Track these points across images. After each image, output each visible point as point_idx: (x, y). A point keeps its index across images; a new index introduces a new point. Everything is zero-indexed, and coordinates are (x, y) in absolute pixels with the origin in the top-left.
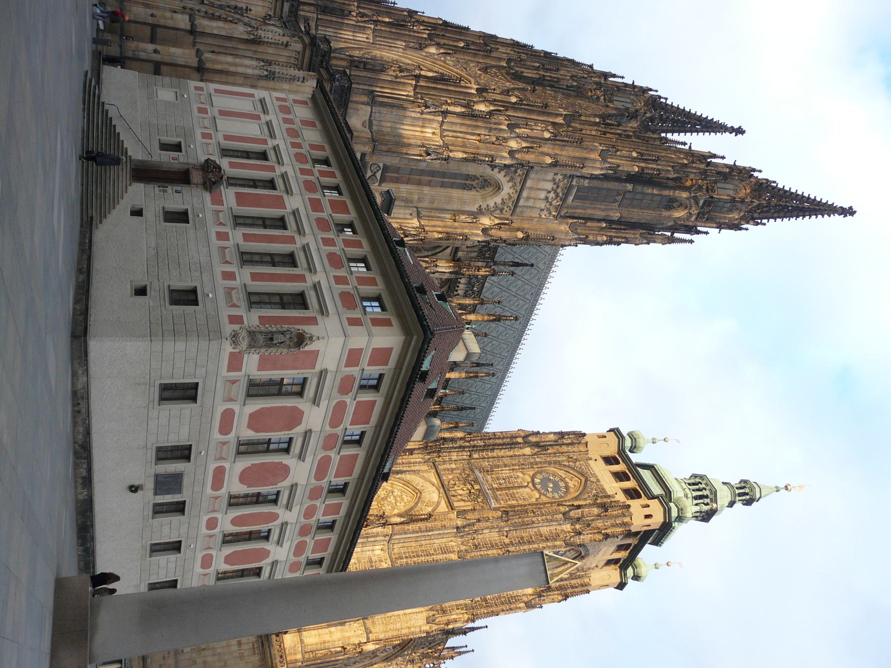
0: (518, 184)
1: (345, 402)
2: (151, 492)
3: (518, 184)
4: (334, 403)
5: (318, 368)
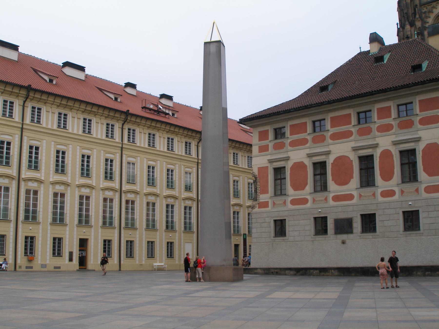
0: (432, 6)
1: (290, 142)
2: (350, 236)
3: (432, 6)
4: (290, 148)
5: (268, 165)
